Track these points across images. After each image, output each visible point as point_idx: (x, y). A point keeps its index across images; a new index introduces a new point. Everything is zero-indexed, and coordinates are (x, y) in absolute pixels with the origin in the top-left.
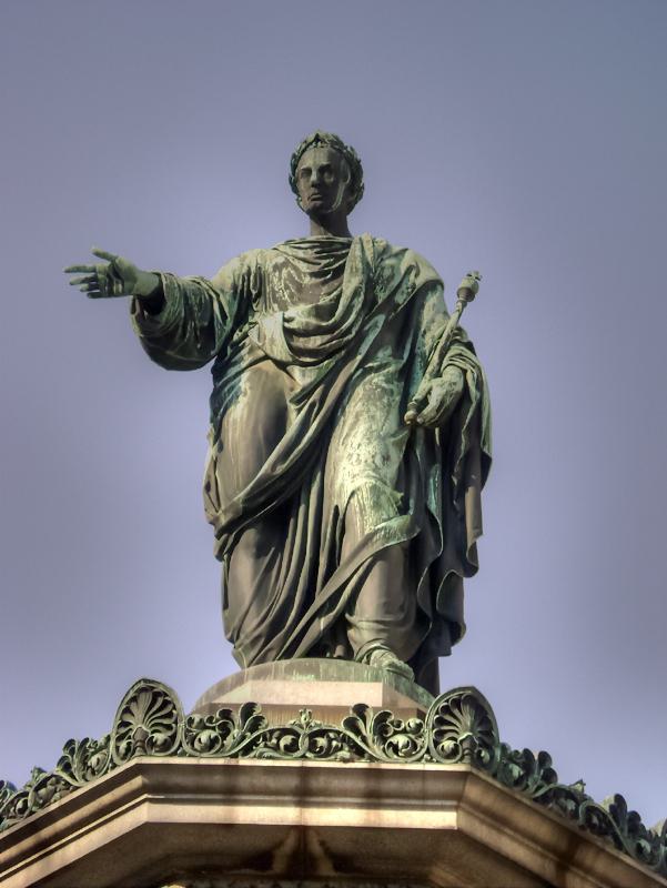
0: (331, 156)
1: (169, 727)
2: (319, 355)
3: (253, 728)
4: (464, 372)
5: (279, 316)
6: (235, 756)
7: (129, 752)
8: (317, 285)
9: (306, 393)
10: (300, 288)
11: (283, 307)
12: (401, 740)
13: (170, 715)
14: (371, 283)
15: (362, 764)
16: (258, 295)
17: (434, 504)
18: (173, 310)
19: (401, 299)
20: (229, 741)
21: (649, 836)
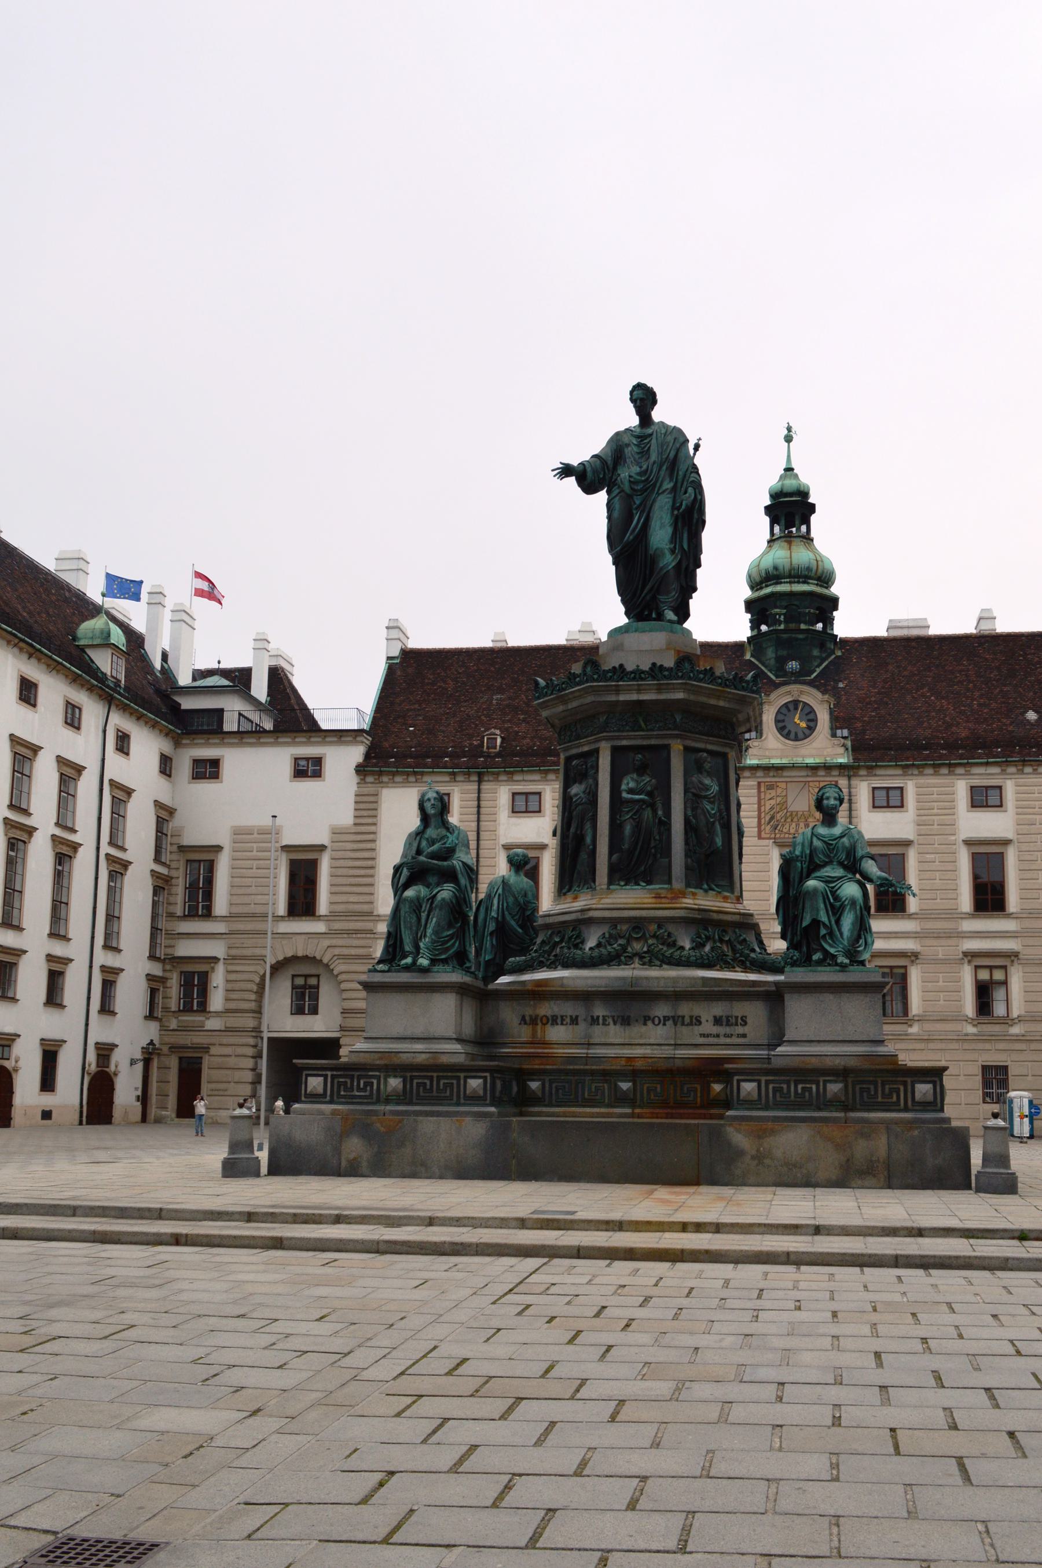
7: (587, 681)
12: (666, 673)
18: (589, 474)
21: (748, 682)
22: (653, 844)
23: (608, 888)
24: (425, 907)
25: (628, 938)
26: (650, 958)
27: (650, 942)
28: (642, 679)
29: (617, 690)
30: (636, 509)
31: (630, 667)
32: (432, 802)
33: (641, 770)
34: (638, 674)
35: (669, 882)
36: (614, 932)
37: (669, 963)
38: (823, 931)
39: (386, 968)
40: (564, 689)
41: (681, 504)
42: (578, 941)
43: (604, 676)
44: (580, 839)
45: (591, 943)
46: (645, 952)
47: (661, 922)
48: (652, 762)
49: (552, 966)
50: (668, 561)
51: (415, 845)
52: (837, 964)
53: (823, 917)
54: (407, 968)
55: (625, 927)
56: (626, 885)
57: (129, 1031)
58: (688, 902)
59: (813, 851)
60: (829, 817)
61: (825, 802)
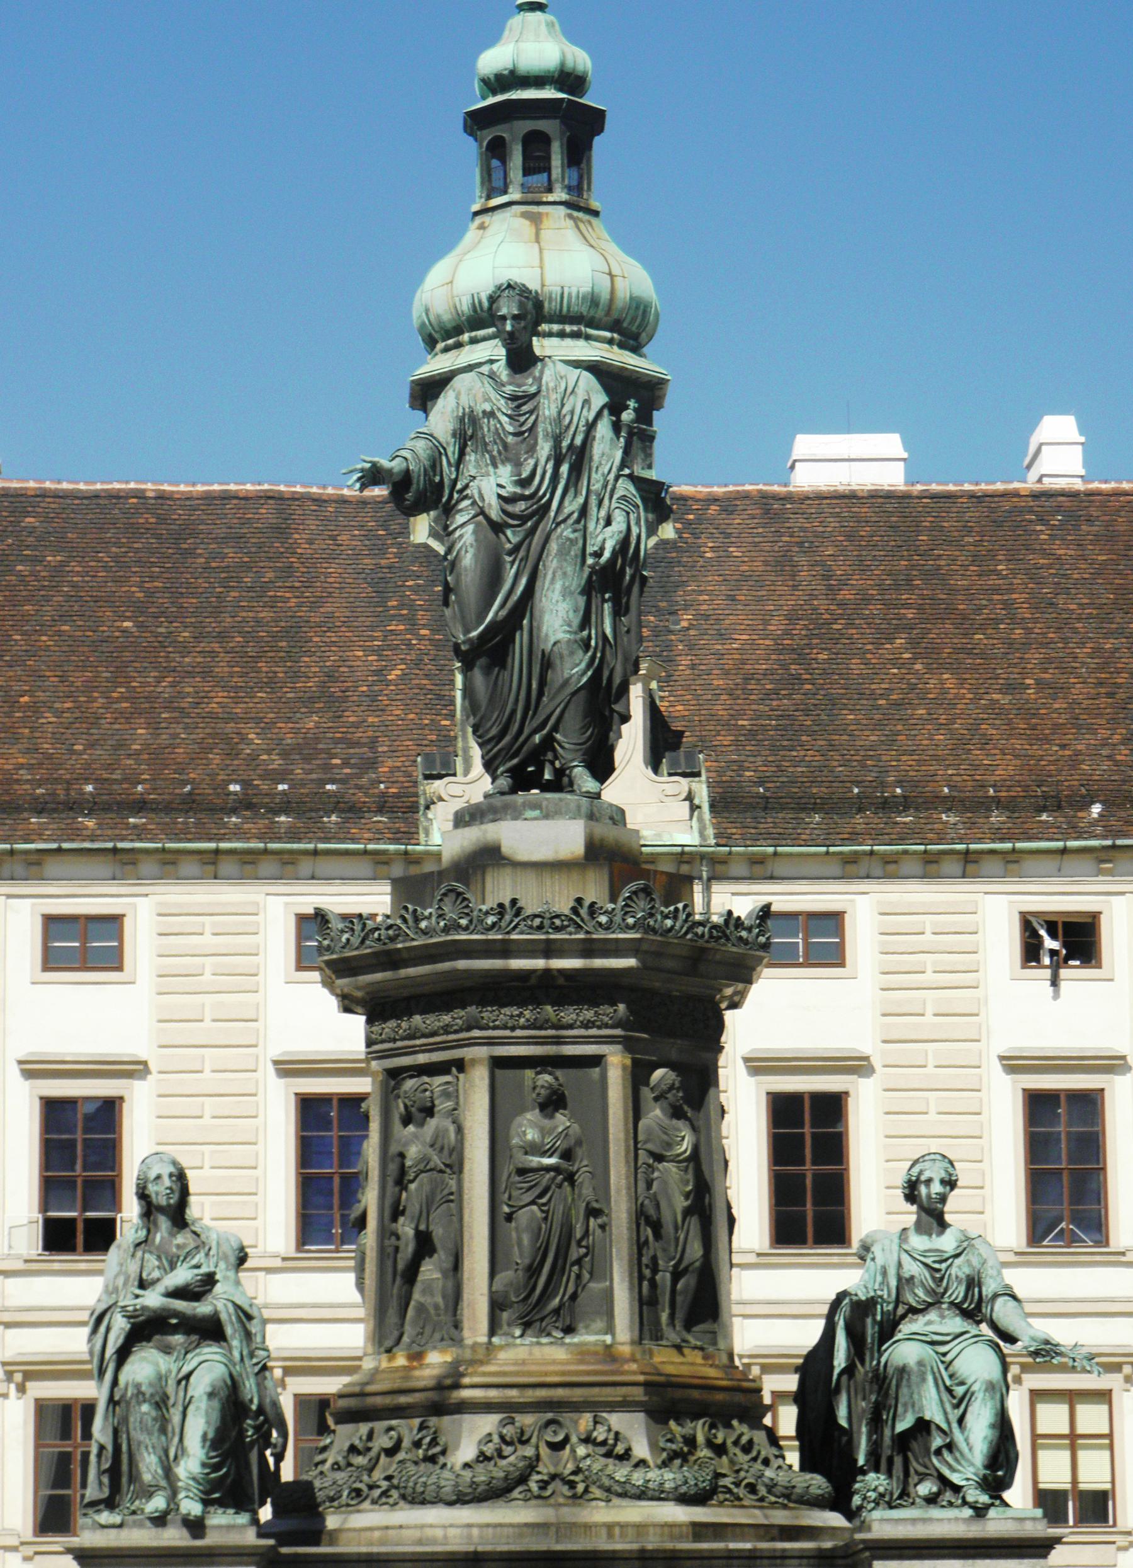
0: (521, 305)
1: (467, 914)
2: (523, 518)
3: (517, 914)
4: (628, 513)
5: (492, 480)
6: (508, 933)
7: (446, 930)
8: (517, 444)
9: (516, 549)
10: (506, 446)
11: (495, 466)
12: (603, 919)
13: (467, 906)
14: (557, 440)
15: (581, 936)
16: (471, 437)
17: (608, 631)
19: (578, 441)
20: (503, 924)
21: (749, 929)
22: (575, 1253)
23: (490, 1343)
27: (581, 1451)
28: (558, 929)
29: (506, 950)
30: (510, 553)
31: (531, 906)
32: (167, 1182)
35: (610, 1329)
36: (509, 1431)
37: (623, 1495)
38: (937, 1441)
39: (116, 1519)
40: (392, 939)
41: (602, 549)
42: (438, 1449)
45: (466, 1452)
46: (574, 1473)
51: (133, 1268)
52: (965, 1503)
54: (160, 1520)
55: (527, 1420)
56: (522, 1336)
59: (906, 1282)
60: (933, 1217)
61: (923, 1190)
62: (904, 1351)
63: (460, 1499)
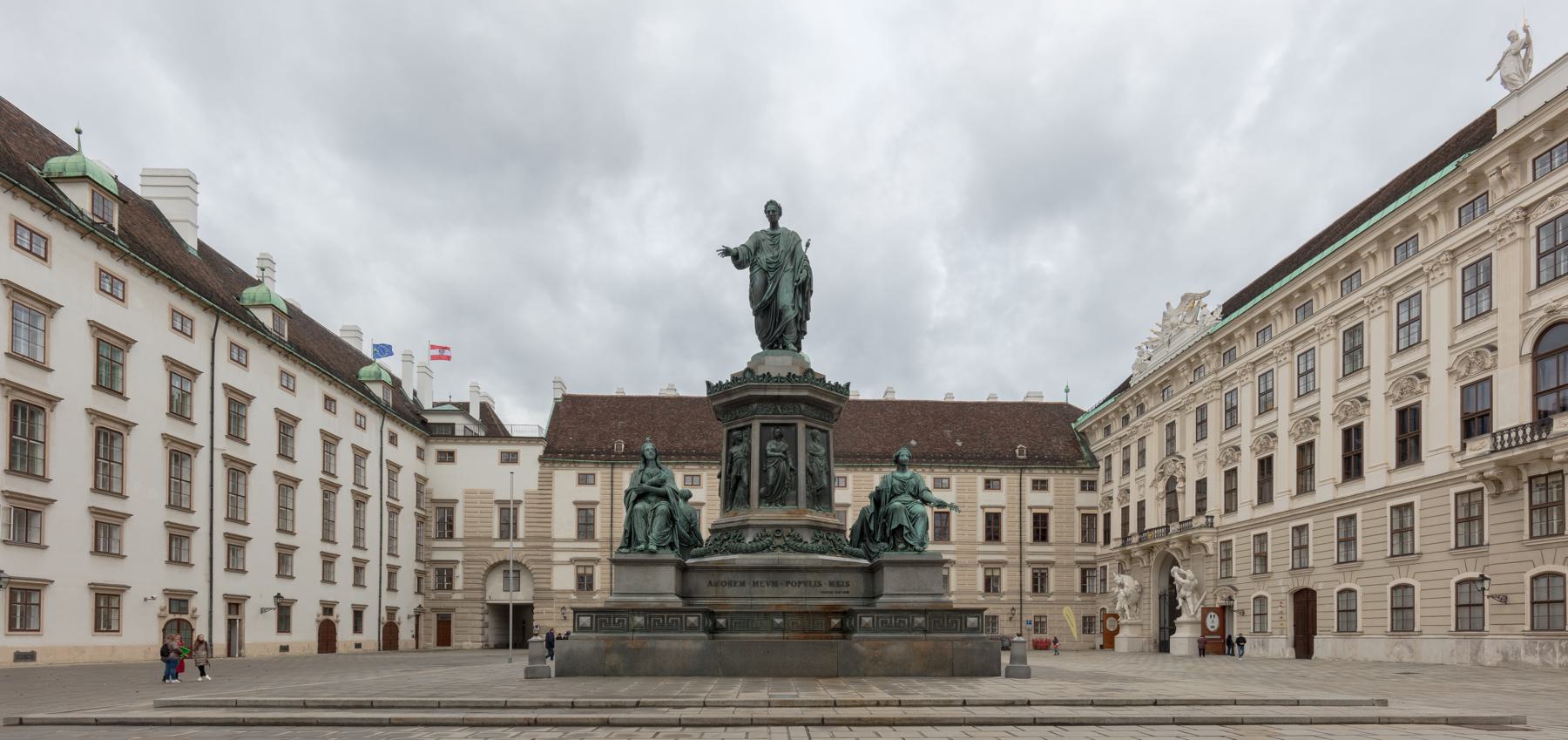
24: (650, 515)
25: (773, 537)
26: (787, 548)
29: (765, 388)
33: (779, 437)
34: (779, 379)
43: (757, 379)
44: (739, 479)
45: (749, 540)
47: (792, 527)
48: (784, 431)
49: (724, 553)
50: (791, 314)
53: (905, 523)
54: (641, 551)
57: (406, 600)
58: (808, 516)
62: (896, 504)
63: (747, 552)
